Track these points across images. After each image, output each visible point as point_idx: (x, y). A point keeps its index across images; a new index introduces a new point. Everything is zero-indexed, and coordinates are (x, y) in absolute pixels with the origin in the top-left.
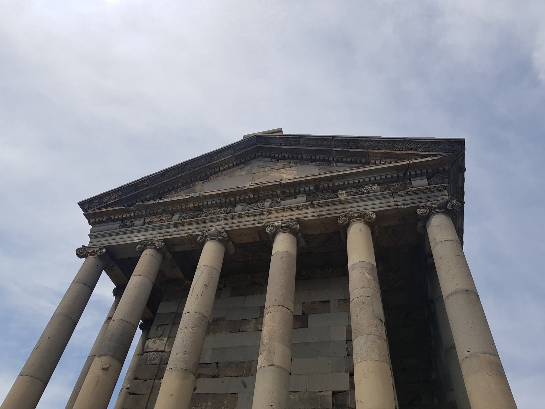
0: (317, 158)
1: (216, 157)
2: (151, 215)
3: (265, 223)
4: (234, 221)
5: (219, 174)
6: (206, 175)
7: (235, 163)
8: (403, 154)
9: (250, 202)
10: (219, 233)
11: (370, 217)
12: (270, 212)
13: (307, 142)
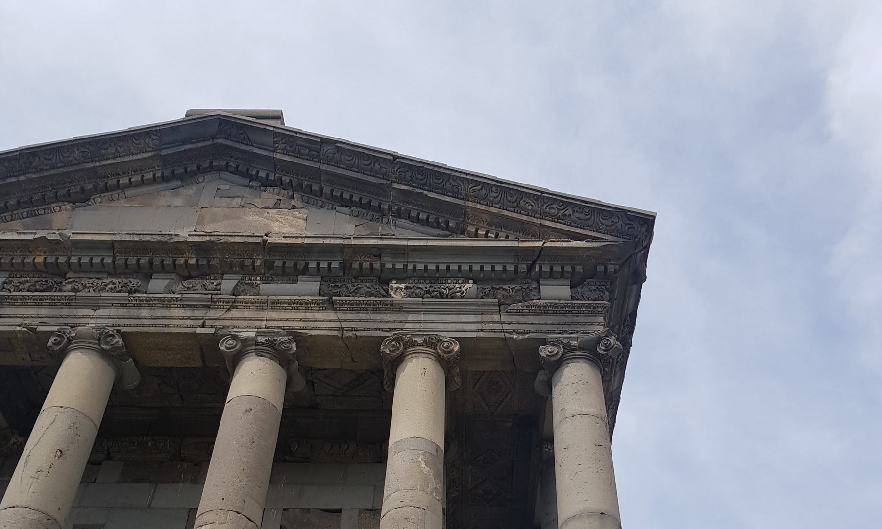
0: (356, 198)
4: (145, 312)
5: (115, 194)
7: (158, 174)
8: (535, 224)
9: (186, 273)
10: (102, 336)
11: (447, 348)
12: (233, 306)
13: (337, 156)
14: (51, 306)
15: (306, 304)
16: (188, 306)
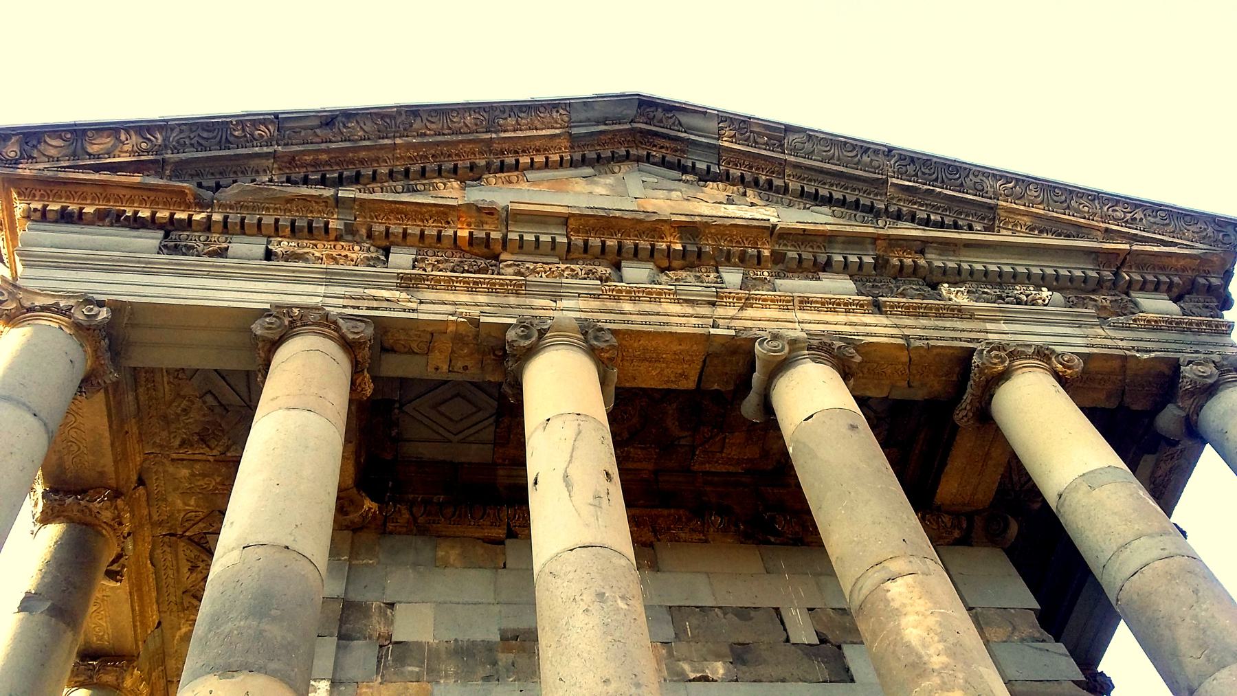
1: (512, 121)
2: (294, 232)
3: (738, 331)
4: (627, 306)
5: (513, 175)
6: (472, 167)
9: (665, 264)
12: (747, 303)
13: (808, 146)
14: (489, 292)
15: (846, 304)
16: (686, 301)
